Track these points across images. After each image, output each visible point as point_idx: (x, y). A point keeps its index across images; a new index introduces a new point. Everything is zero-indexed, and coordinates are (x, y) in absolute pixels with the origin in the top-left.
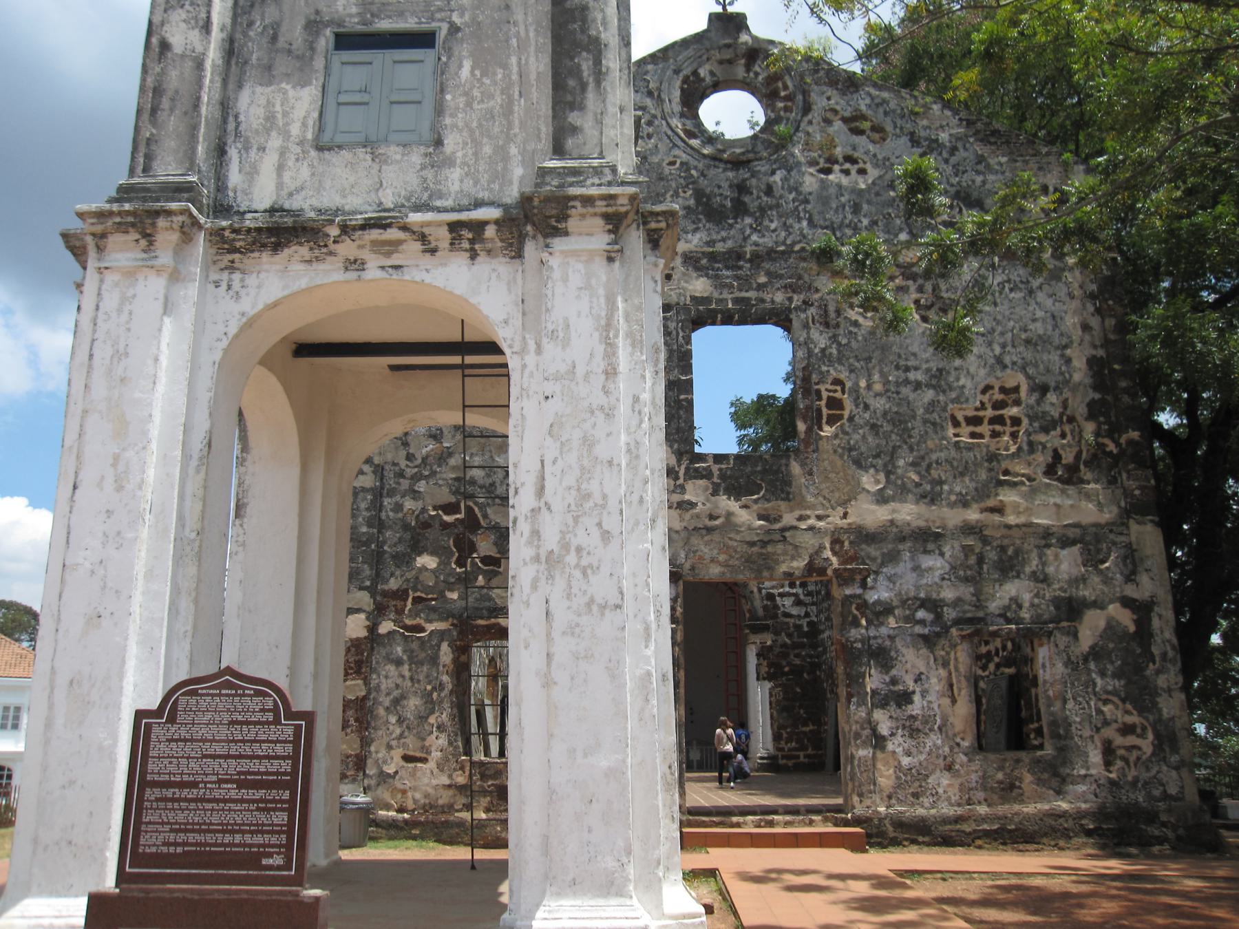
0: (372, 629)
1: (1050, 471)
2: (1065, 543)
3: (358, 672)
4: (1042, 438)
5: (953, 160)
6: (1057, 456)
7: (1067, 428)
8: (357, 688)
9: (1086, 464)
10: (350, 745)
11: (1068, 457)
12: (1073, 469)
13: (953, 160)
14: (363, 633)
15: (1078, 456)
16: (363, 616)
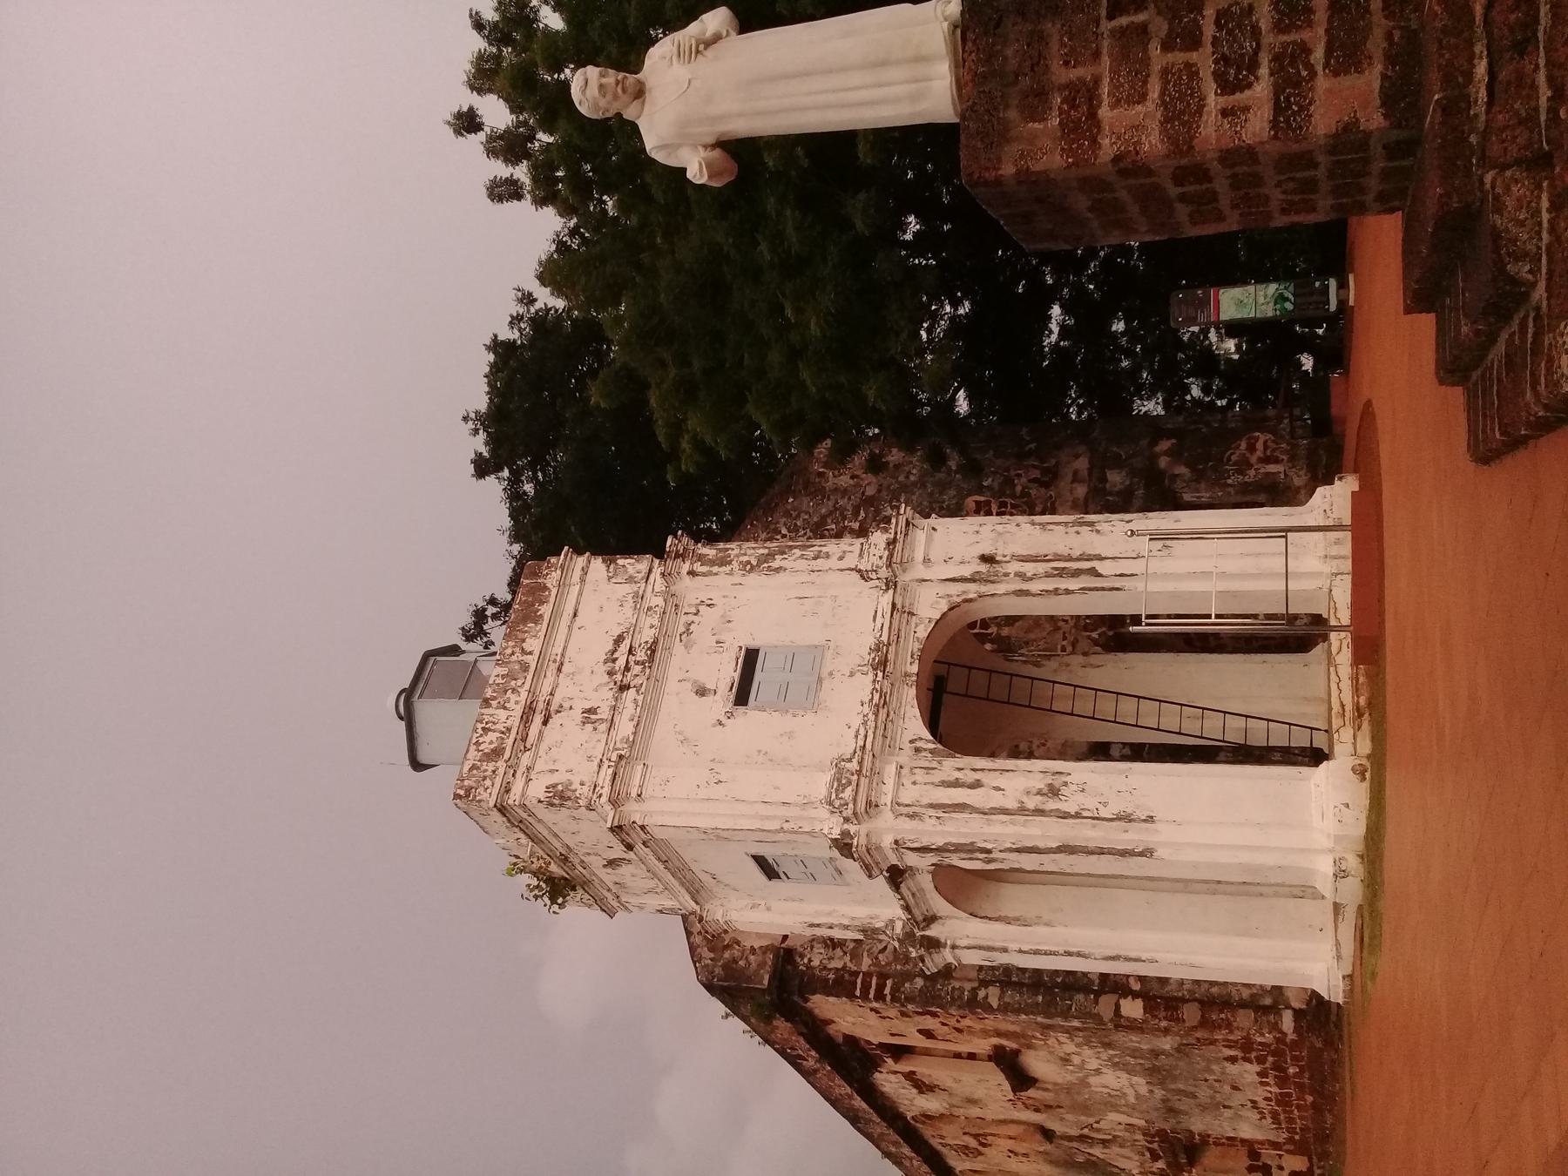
0: (1135, 995)
1: (1046, 485)
2: (1104, 480)
3: (1176, 1008)
4: (1019, 488)
5: (784, 531)
6: (1034, 480)
7: (1013, 473)
8: (1191, 1013)
9: (1042, 461)
10: (1244, 1019)
11: (1036, 474)
12: (1045, 471)
13: (784, 531)
14: (1139, 1003)
15: (1035, 467)
16: (1122, 1002)
